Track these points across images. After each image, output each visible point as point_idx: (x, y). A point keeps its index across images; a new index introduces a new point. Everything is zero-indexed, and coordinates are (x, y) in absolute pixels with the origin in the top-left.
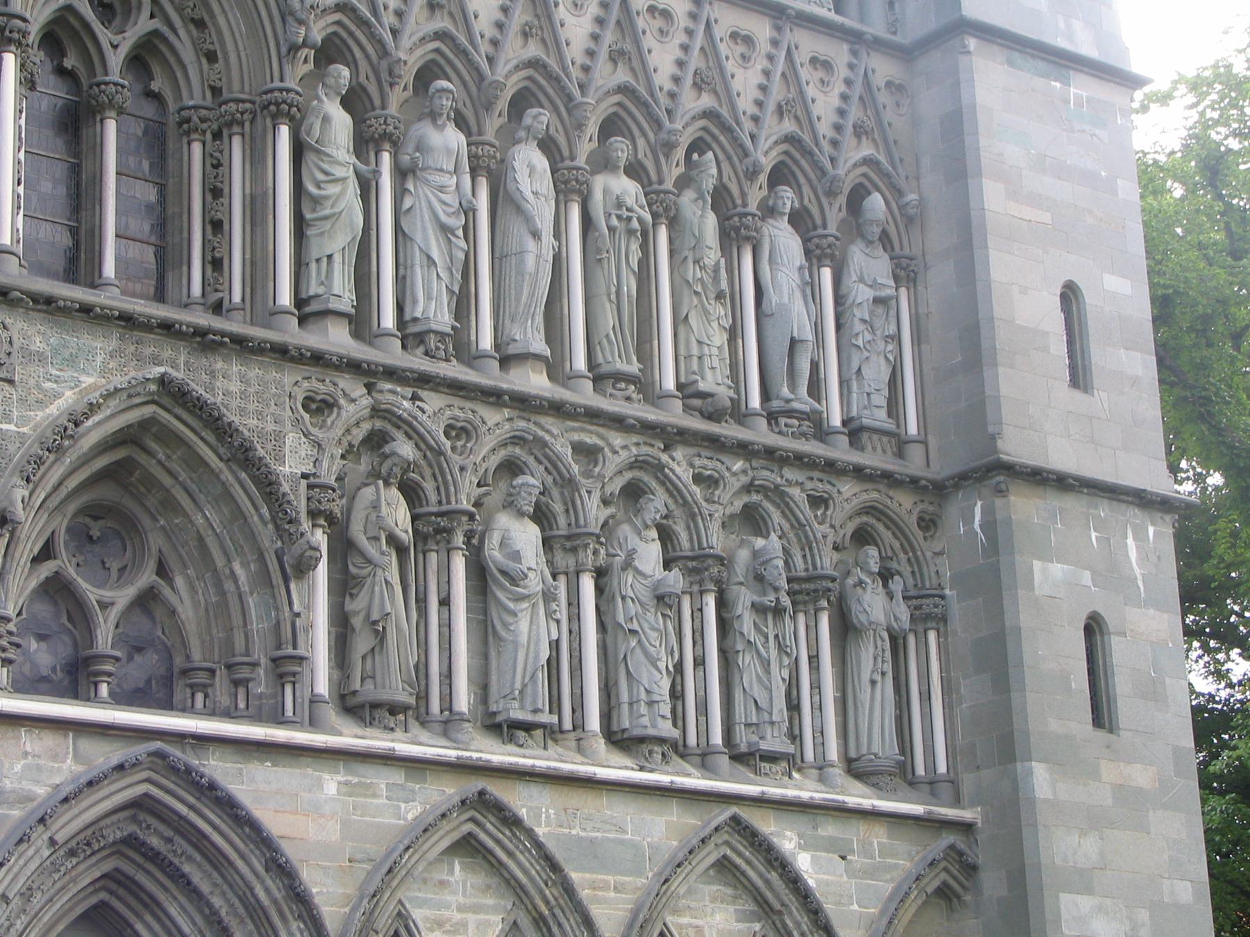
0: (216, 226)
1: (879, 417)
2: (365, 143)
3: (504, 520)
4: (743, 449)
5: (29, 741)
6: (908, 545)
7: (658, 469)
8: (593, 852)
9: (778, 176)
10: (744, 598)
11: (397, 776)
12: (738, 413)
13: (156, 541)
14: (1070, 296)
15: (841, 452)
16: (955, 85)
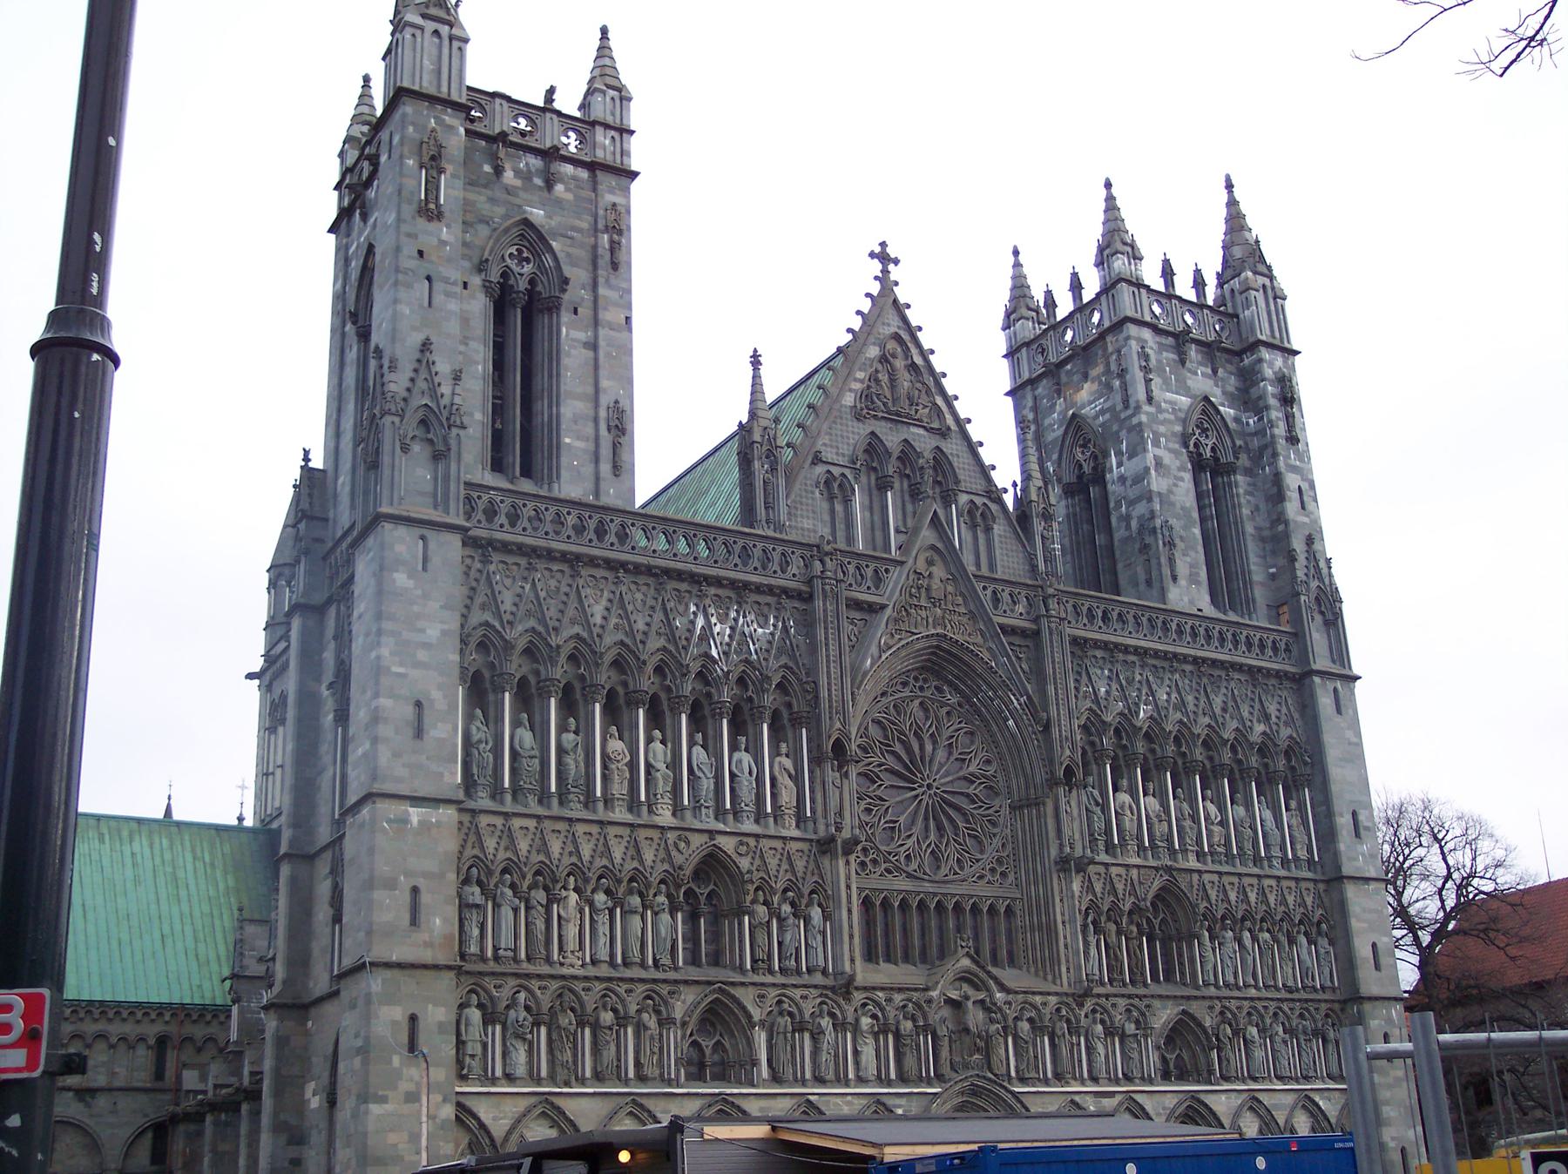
0: (1181, 964)
1: (1329, 984)
2: (1212, 939)
3: (1249, 1028)
4: (1299, 1000)
5: (1169, 1095)
6: (1338, 1017)
7: (1280, 1008)
8: (1276, 1106)
9: (1301, 922)
10: (1302, 1037)
11: (1235, 1094)
12: (1297, 990)
13: (1178, 1042)
14: (1374, 945)
15: (1321, 996)
16: (1342, 893)
